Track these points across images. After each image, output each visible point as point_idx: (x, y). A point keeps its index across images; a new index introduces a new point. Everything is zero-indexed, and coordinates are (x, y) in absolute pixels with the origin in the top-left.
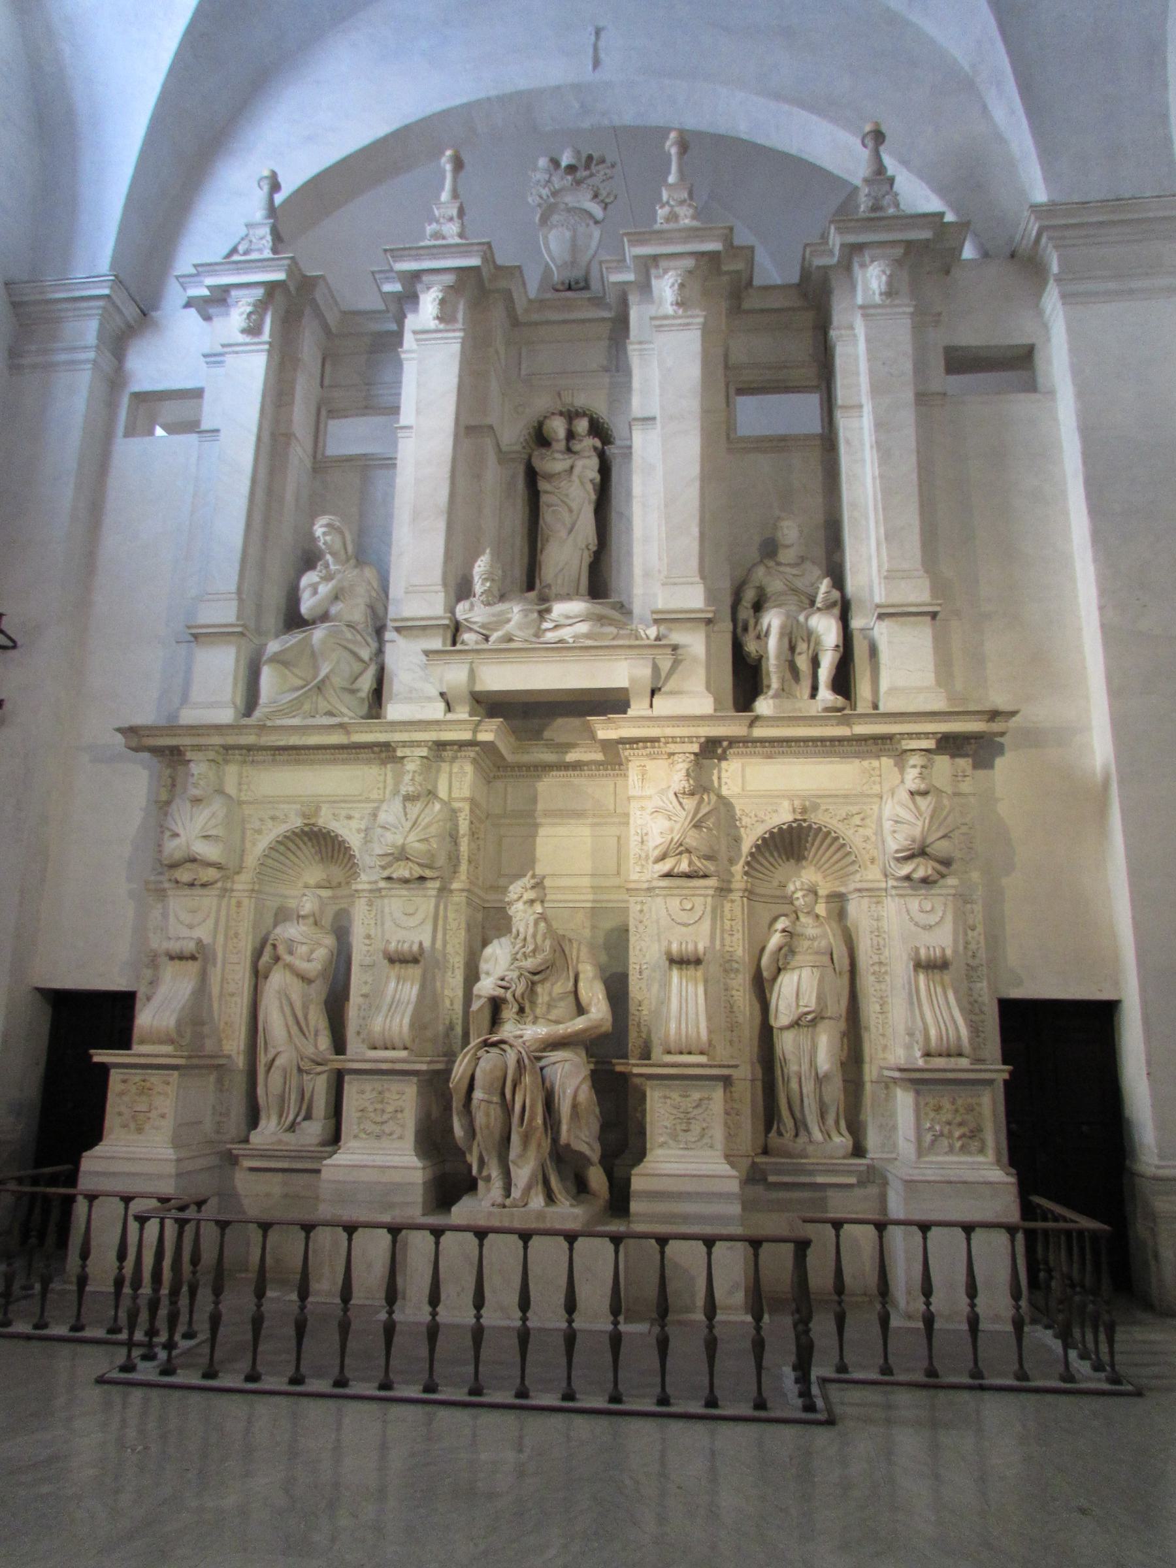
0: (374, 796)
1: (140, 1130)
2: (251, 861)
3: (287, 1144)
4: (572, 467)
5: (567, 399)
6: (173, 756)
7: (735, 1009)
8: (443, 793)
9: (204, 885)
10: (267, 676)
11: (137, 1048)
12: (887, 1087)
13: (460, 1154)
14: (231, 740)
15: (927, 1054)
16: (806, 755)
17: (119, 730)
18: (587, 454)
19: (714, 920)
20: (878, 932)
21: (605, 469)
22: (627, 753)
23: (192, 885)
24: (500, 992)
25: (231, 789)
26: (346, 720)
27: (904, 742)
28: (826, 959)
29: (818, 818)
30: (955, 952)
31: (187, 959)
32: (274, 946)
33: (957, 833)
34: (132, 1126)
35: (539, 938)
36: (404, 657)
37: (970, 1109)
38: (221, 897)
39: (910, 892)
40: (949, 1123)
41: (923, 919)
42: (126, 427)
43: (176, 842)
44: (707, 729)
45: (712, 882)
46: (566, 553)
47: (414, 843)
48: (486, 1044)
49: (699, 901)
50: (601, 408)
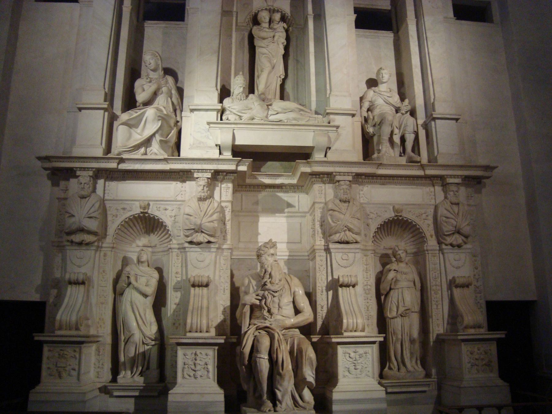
1: (60, 377)
4: (274, 37)
7: (370, 309)
16: (400, 184)
17: (39, 158)
18: (279, 30)
22: (313, 179)
27: (448, 179)
28: (412, 284)
32: (128, 277)
38: (96, 251)
43: (73, 220)
44: (357, 169)
47: (206, 223)
49: (351, 255)
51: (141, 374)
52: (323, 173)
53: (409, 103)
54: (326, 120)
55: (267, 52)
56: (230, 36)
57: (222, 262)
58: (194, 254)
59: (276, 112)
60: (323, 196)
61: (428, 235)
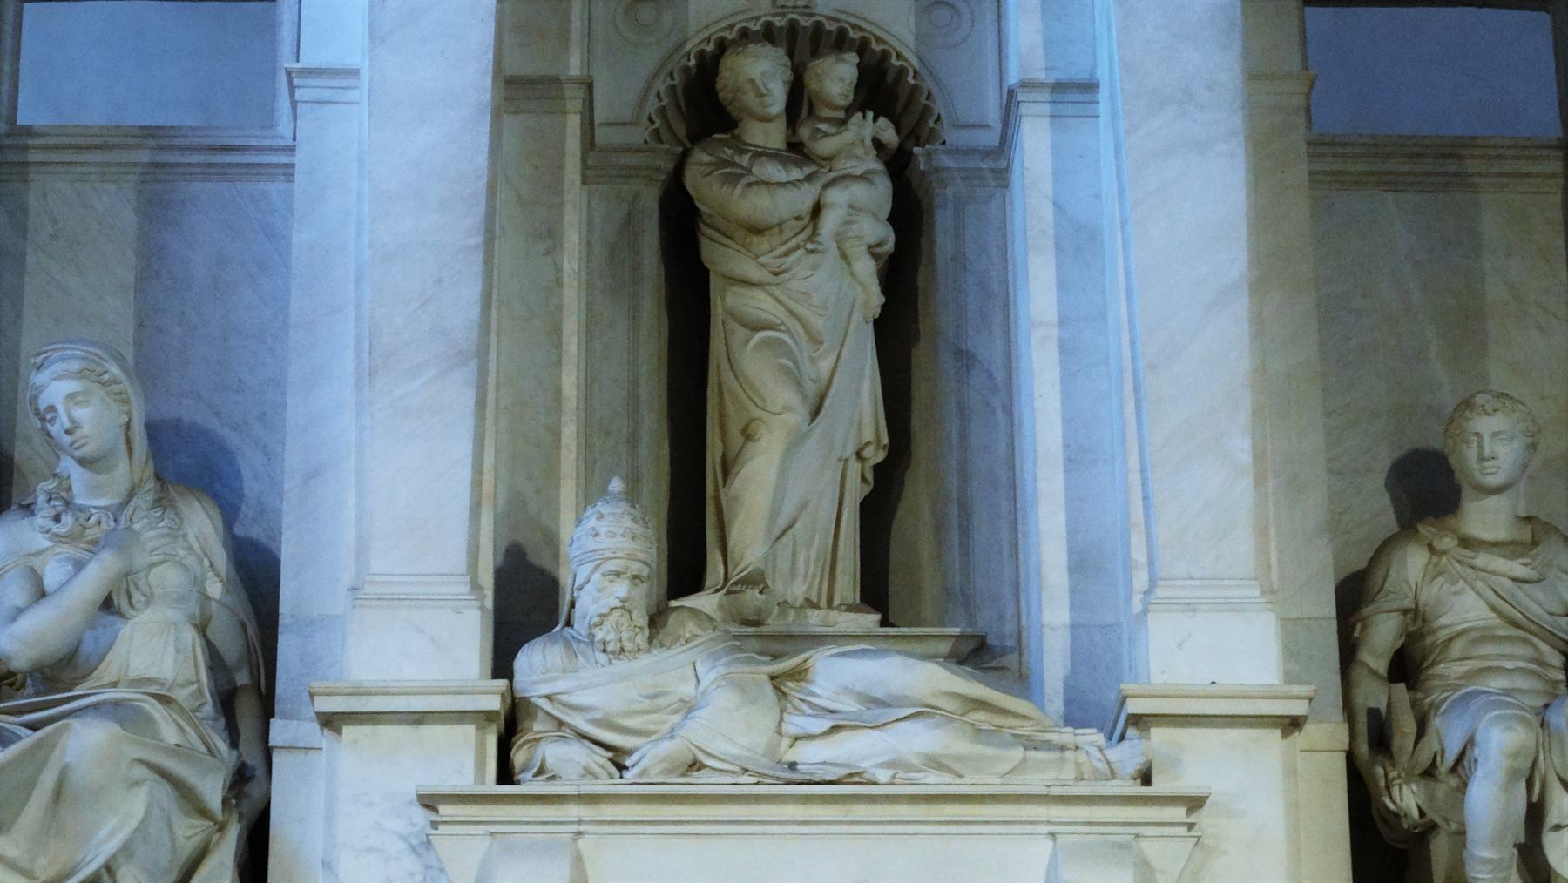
4: (817, 210)
54: (1128, 756)
55: (779, 314)
56: (550, 236)
59: (826, 724)
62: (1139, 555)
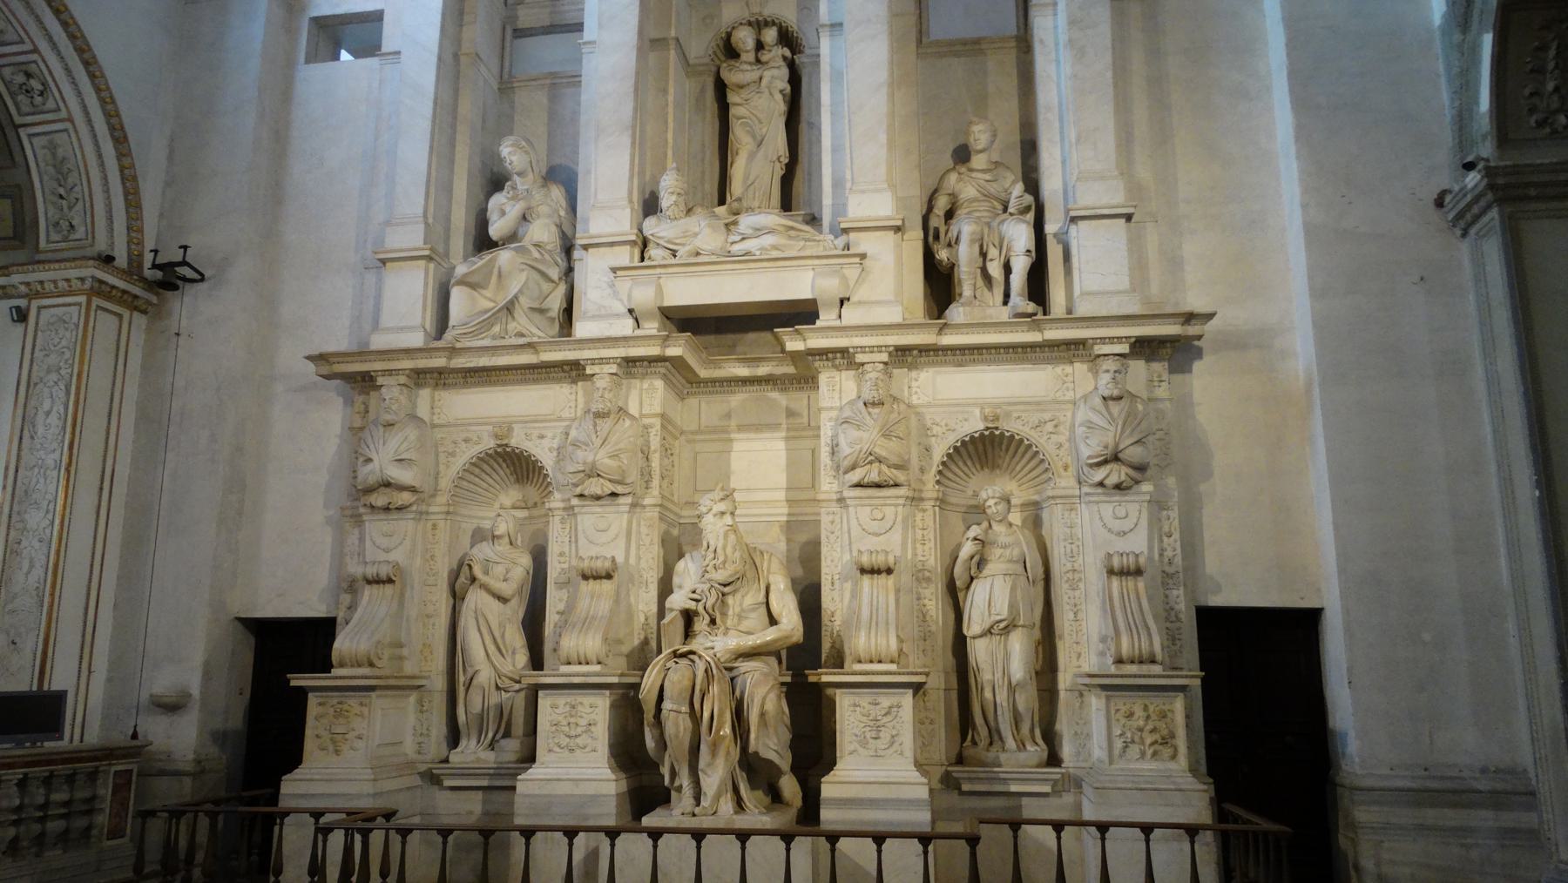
0: (566, 414)
1: (337, 752)
2: (445, 483)
3: (486, 762)
5: (756, 10)
6: (365, 382)
8: (633, 409)
9: (399, 509)
10: (458, 297)
11: (335, 672)
12: (1081, 695)
13: (655, 766)
14: (422, 363)
15: (1119, 661)
17: (309, 358)
19: (905, 529)
20: (1071, 539)
21: (795, 80)
23: (387, 509)
24: (692, 605)
25: (423, 411)
26: (535, 339)
28: (1020, 569)
29: (1010, 426)
30: (1150, 559)
31: (384, 582)
33: (1151, 438)
34: (331, 748)
35: (729, 550)
36: (593, 271)
37: (1163, 715)
39: (1103, 498)
40: (1141, 730)
41: (1117, 525)
42: (307, 53)
43: (370, 467)
45: (902, 491)
46: (757, 165)
48: (676, 655)
49: (889, 511)
50: (790, 17)
51: (492, 746)
52: (834, 351)
53: (1027, 190)
56: (665, 91)
57: (644, 530)
58: (590, 518)
60: (837, 395)
61: (1058, 465)
62: (848, 176)
